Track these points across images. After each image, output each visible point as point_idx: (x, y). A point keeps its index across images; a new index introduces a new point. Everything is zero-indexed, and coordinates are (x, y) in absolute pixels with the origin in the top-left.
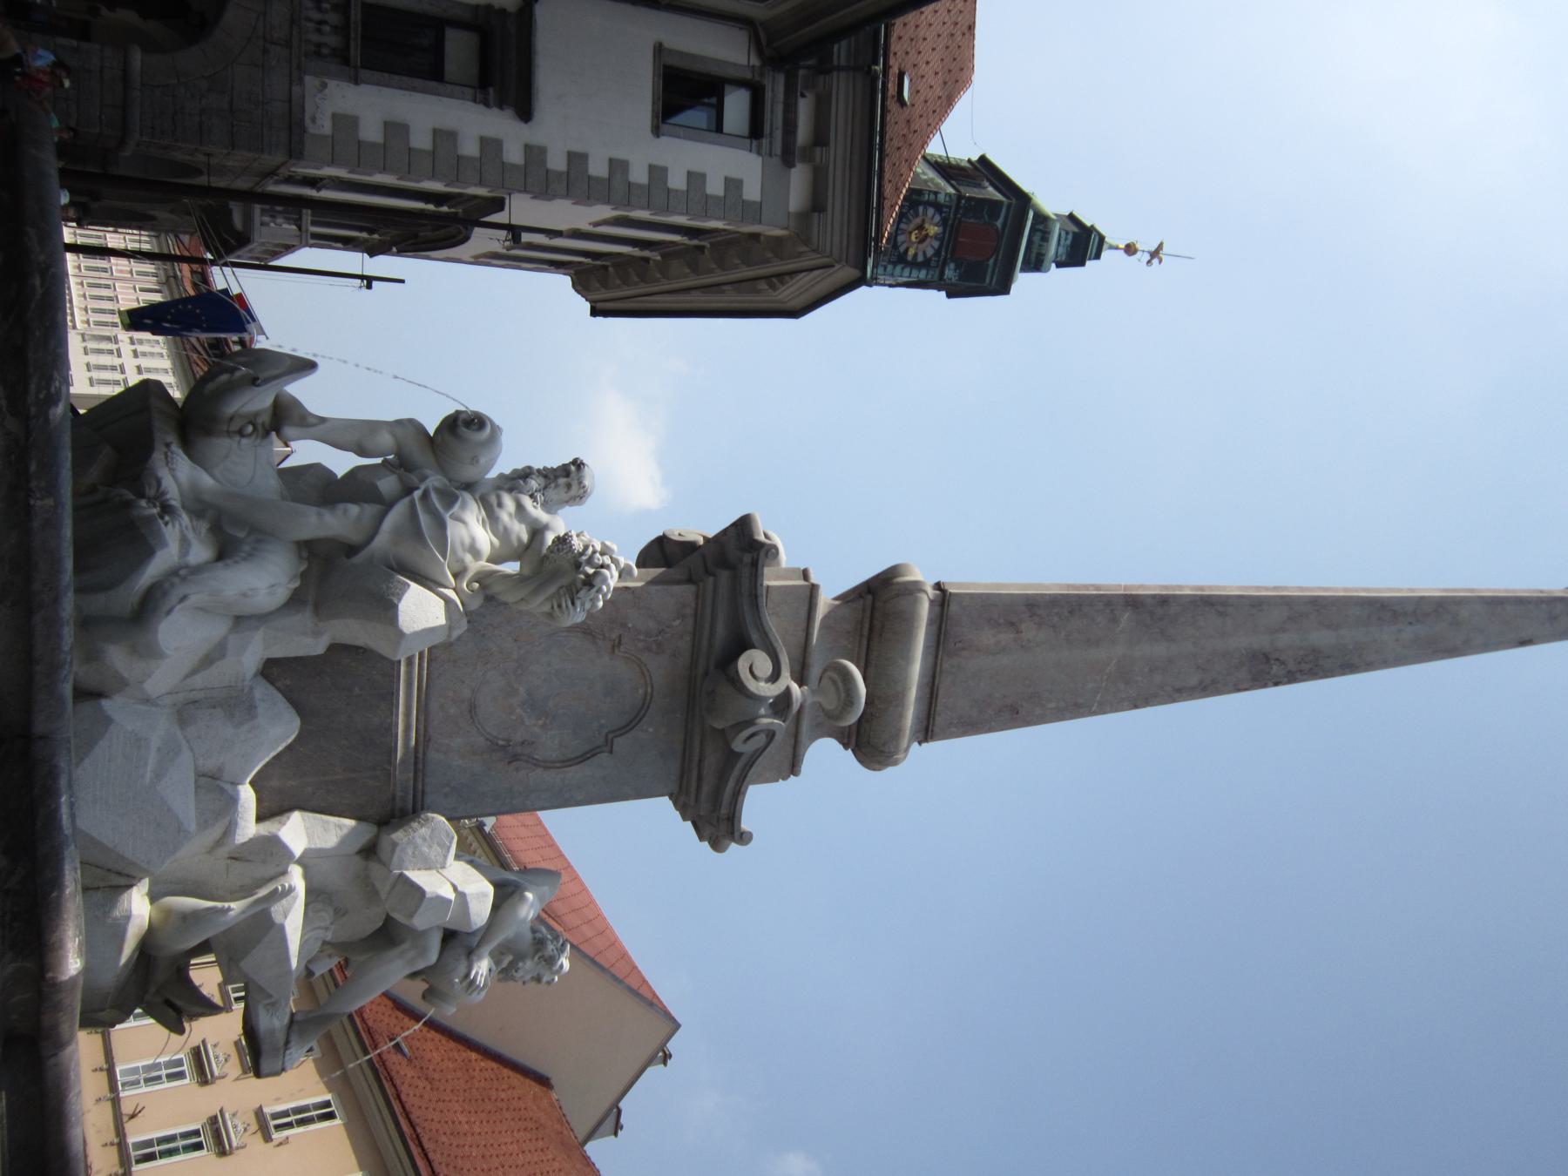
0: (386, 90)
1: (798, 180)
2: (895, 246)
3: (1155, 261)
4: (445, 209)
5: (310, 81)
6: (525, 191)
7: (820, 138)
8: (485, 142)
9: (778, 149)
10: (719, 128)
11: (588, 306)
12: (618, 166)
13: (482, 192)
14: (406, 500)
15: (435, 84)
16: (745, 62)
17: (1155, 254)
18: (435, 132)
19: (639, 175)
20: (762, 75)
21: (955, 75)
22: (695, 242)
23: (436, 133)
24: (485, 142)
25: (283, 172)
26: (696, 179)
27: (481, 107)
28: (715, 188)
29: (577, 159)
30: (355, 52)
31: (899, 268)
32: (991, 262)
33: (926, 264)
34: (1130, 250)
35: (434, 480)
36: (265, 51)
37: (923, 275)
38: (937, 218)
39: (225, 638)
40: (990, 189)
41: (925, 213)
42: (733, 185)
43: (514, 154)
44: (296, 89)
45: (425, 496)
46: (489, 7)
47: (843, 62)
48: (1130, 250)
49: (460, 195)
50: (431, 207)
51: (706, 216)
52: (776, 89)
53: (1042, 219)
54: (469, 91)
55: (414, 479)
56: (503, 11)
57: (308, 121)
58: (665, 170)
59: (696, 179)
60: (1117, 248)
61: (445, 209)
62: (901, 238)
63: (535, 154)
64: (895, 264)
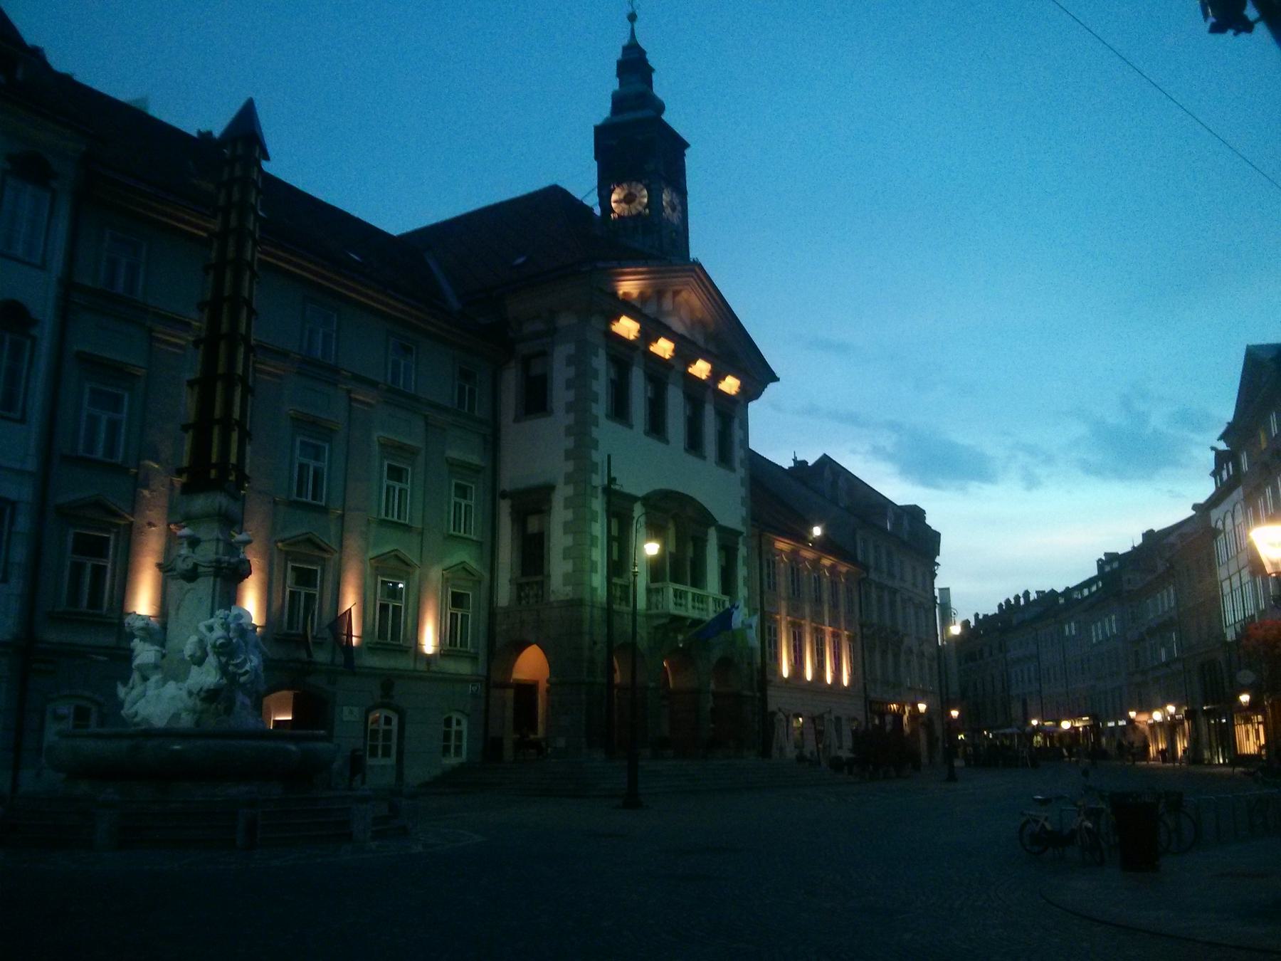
5: (552, 598)
8: (566, 507)
11: (772, 387)
12: (569, 431)
19: (570, 419)
23: (565, 533)
24: (566, 507)
26: (569, 384)
28: (571, 372)
30: (539, 578)
34: (632, 18)
42: (570, 361)
43: (569, 491)
46: (511, 514)
48: (632, 18)
56: (512, 506)
59: (569, 384)
63: (569, 479)
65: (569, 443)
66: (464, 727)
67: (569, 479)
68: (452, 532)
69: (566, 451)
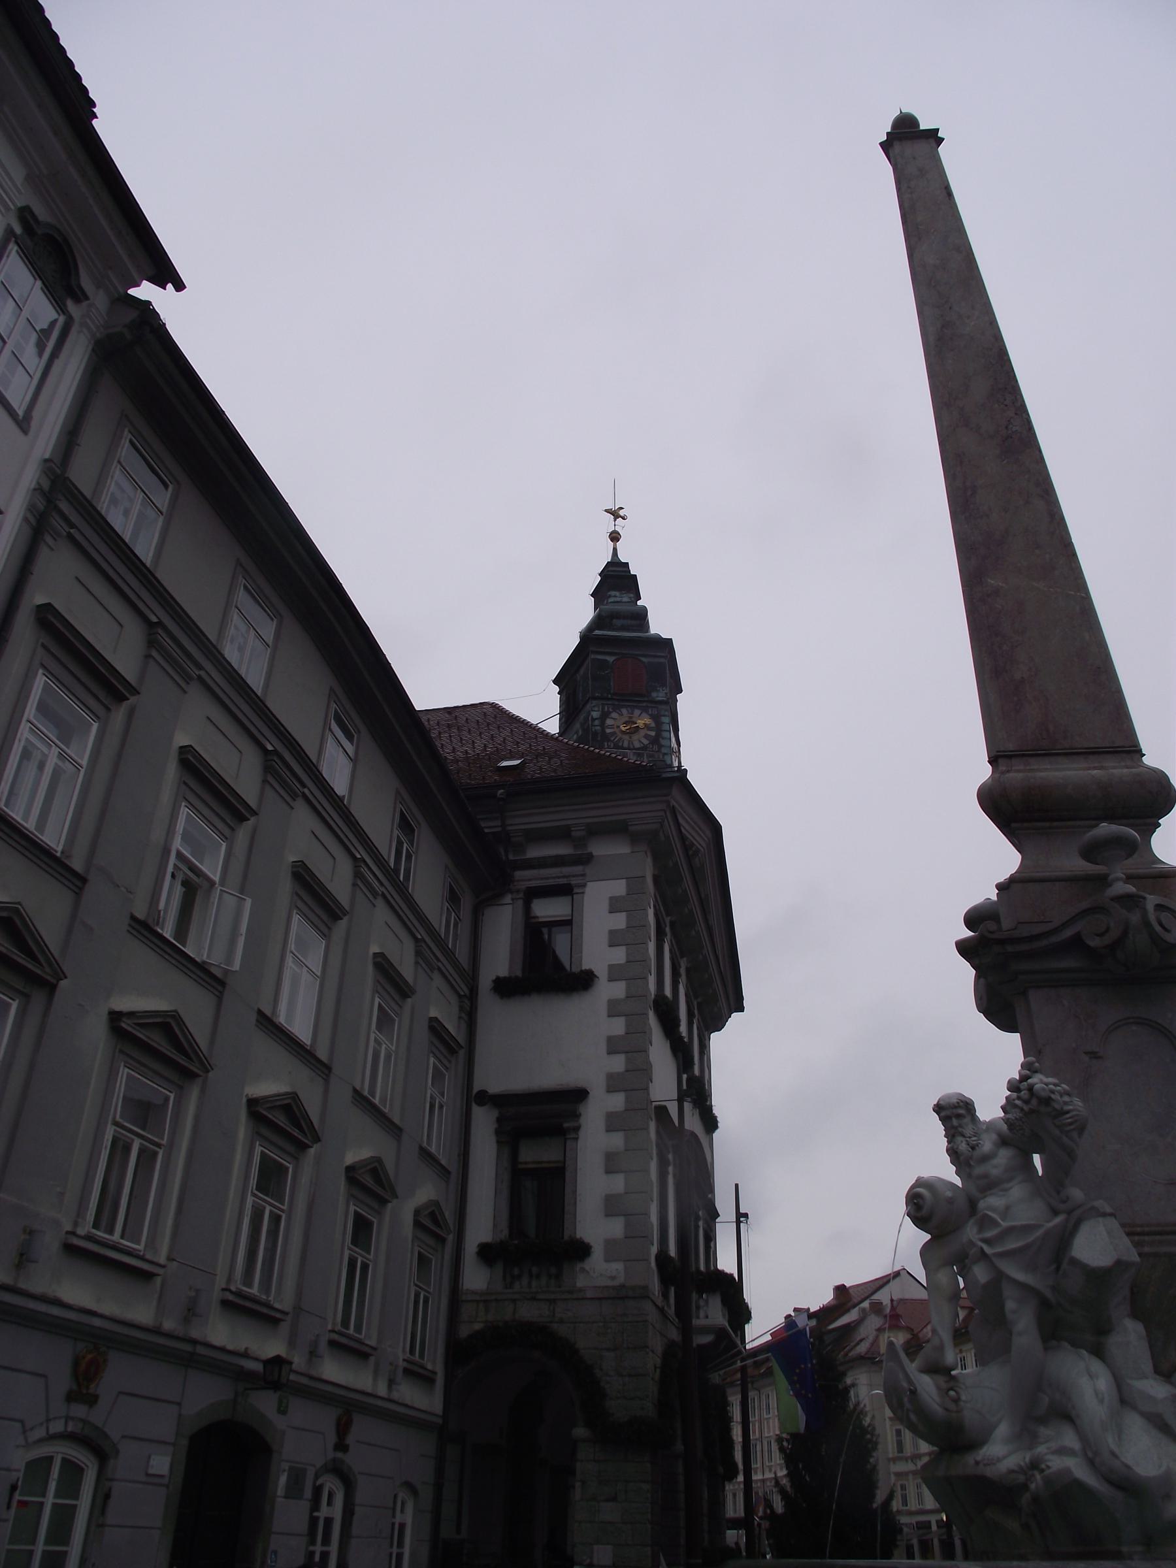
0: (578, 1219)
1: (601, 849)
2: (645, 748)
3: (621, 513)
4: (670, 1157)
6: (647, 1089)
7: (562, 834)
8: (609, 1129)
9: (578, 869)
10: (567, 923)
13: (652, 1126)
14: (994, 1259)
15: (568, 1175)
16: (510, 907)
17: (615, 514)
18: (608, 1171)
20: (518, 891)
21: (491, 717)
22: (668, 929)
24: (609, 1129)
25: (660, 1301)
26: (615, 939)
27: (582, 1133)
28: (619, 921)
29: (613, 1046)
31: (663, 742)
32: (644, 659)
33: (656, 718)
34: (615, 537)
35: (970, 1232)
36: (561, 1321)
37: (666, 720)
38: (614, 715)
39: (1143, 1414)
40: (582, 671)
41: (612, 726)
42: (615, 906)
43: (617, 1102)
44: (589, 1295)
45: (987, 1241)
46: (498, 1132)
47: (499, 823)
48: (615, 537)
49: (658, 1145)
50: (671, 1169)
51: (645, 926)
52: (526, 878)
53: (598, 622)
54: (569, 1143)
55: (973, 1251)
56: (499, 1120)
57: (616, 1283)
58: (611, 967)
59: (615, 939)
60: (615, 550)
61: (670, 1157)
62: (637, 745)
63: (614, 1084)
64: (661, 746)
65: (618, 1027)
66: (408, 1518)
67: (614, 1084)
68: (425, 1145)
69: (611, 1040)
